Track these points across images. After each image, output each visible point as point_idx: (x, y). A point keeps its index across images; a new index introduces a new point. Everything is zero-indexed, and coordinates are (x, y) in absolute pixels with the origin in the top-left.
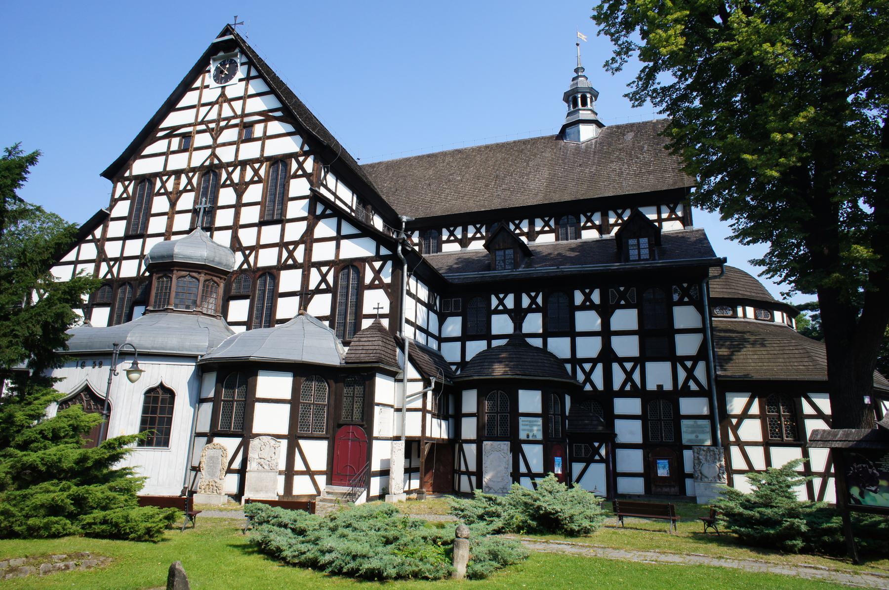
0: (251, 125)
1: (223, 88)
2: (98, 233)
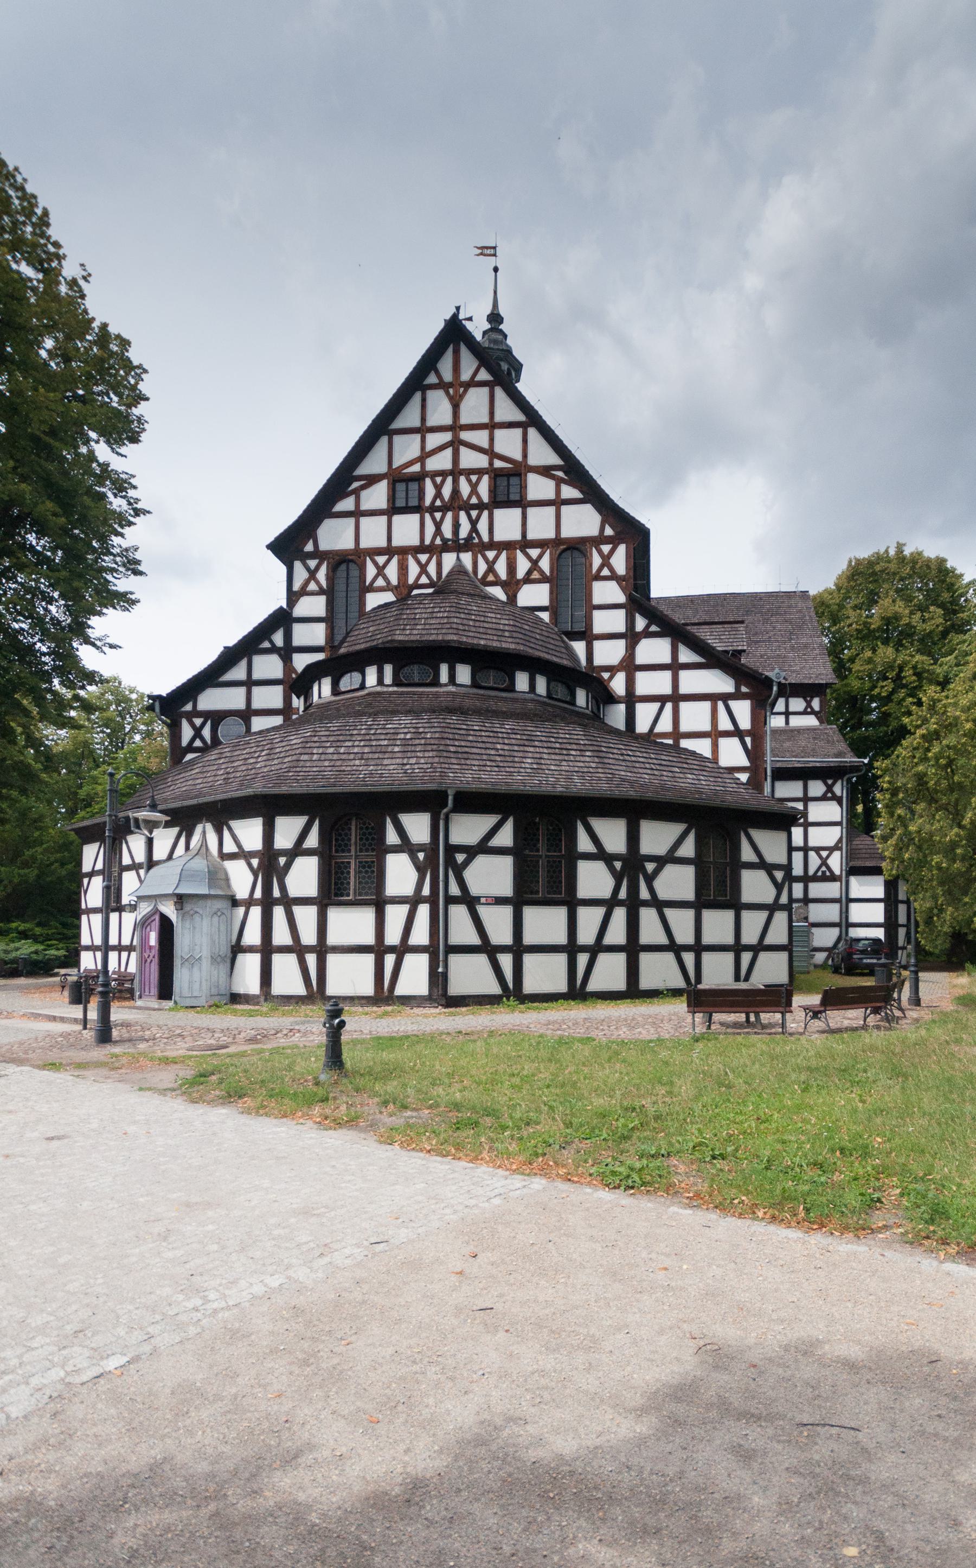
2: (278, 638)
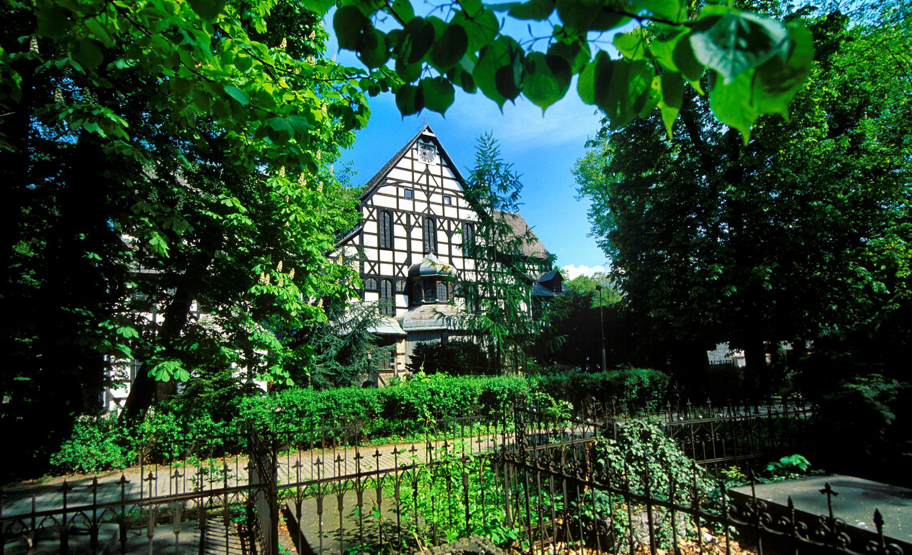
0: (449, 197)
1: (427, 165)
2: (356, 240)
